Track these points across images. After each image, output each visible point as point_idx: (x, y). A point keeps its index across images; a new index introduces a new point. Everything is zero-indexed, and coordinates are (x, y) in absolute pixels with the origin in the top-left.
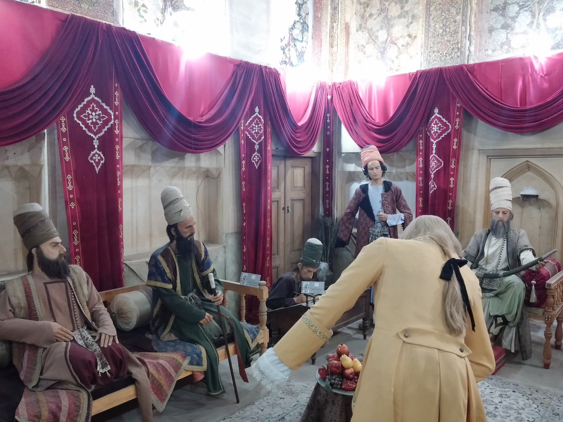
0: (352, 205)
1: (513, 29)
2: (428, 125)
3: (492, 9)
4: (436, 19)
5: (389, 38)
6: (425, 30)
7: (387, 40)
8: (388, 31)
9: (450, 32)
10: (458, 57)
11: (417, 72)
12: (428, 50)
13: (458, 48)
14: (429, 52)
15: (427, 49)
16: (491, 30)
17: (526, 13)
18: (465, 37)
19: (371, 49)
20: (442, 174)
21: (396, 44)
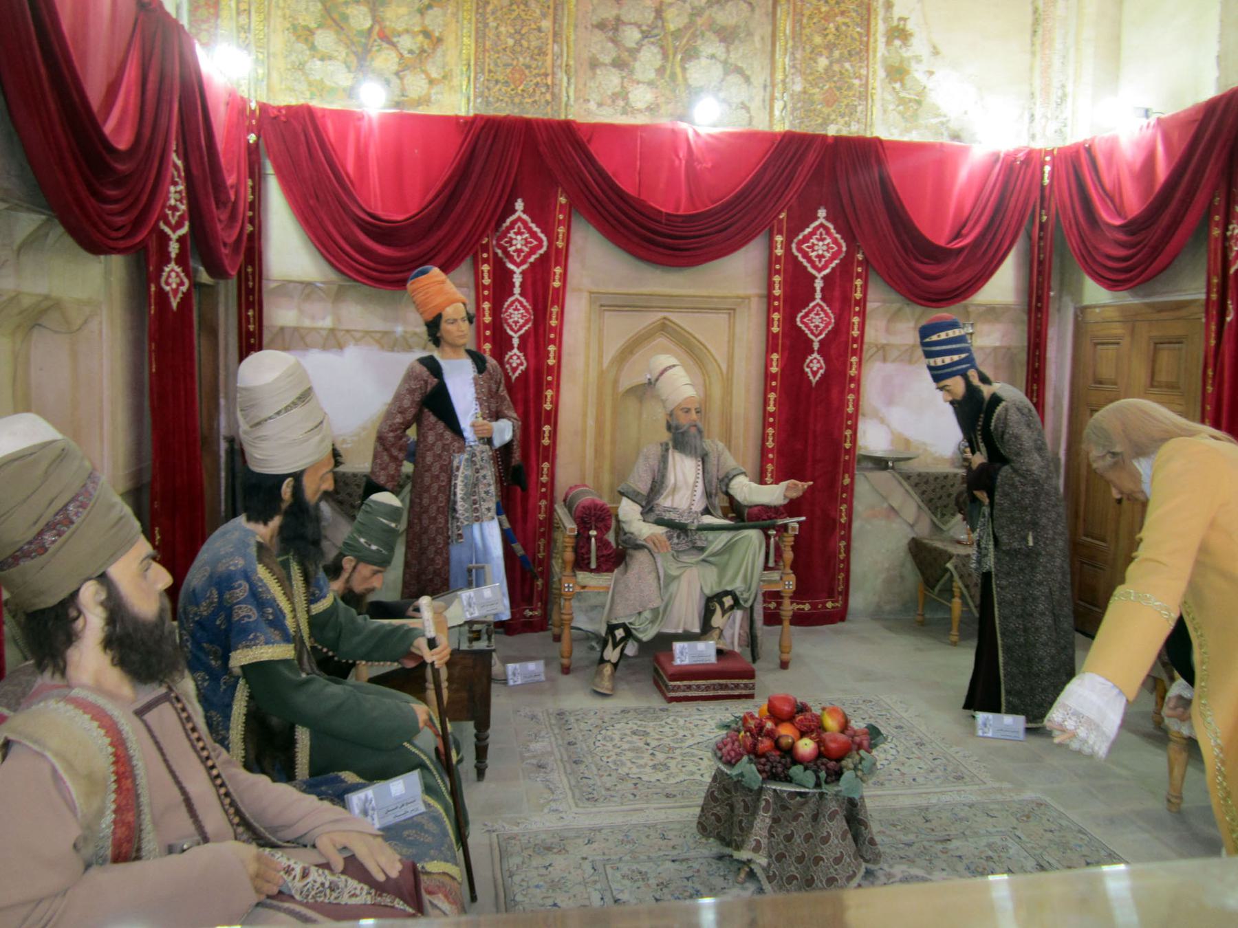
0: (407, 403)
1: (632, 72)
2: (498, 234)
3: (595, 23)
4: (499, 13)
5: (377, 28)
6: (477, 32)
7: (371, 29)
8: (373, 11)
9: (528, 48)
10: (547, 103)
11: (476, 117)
12: (483, 74)
13: (547, 85)
14: (488, 80)
15: (483, 72)
16: (594, 64)
17: (652, 48)
18: (560, 66)
19: (325, 39)
20: (531, 340)
21: (394, 45)
